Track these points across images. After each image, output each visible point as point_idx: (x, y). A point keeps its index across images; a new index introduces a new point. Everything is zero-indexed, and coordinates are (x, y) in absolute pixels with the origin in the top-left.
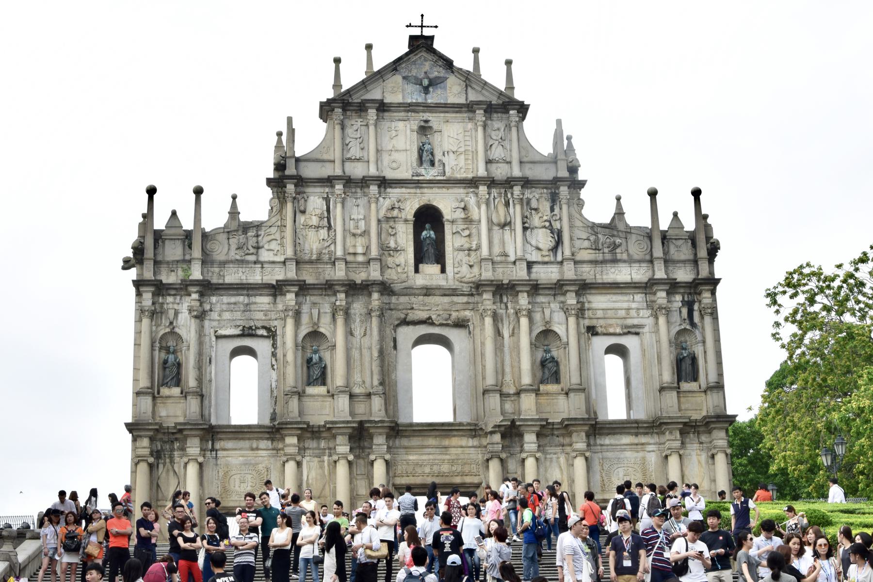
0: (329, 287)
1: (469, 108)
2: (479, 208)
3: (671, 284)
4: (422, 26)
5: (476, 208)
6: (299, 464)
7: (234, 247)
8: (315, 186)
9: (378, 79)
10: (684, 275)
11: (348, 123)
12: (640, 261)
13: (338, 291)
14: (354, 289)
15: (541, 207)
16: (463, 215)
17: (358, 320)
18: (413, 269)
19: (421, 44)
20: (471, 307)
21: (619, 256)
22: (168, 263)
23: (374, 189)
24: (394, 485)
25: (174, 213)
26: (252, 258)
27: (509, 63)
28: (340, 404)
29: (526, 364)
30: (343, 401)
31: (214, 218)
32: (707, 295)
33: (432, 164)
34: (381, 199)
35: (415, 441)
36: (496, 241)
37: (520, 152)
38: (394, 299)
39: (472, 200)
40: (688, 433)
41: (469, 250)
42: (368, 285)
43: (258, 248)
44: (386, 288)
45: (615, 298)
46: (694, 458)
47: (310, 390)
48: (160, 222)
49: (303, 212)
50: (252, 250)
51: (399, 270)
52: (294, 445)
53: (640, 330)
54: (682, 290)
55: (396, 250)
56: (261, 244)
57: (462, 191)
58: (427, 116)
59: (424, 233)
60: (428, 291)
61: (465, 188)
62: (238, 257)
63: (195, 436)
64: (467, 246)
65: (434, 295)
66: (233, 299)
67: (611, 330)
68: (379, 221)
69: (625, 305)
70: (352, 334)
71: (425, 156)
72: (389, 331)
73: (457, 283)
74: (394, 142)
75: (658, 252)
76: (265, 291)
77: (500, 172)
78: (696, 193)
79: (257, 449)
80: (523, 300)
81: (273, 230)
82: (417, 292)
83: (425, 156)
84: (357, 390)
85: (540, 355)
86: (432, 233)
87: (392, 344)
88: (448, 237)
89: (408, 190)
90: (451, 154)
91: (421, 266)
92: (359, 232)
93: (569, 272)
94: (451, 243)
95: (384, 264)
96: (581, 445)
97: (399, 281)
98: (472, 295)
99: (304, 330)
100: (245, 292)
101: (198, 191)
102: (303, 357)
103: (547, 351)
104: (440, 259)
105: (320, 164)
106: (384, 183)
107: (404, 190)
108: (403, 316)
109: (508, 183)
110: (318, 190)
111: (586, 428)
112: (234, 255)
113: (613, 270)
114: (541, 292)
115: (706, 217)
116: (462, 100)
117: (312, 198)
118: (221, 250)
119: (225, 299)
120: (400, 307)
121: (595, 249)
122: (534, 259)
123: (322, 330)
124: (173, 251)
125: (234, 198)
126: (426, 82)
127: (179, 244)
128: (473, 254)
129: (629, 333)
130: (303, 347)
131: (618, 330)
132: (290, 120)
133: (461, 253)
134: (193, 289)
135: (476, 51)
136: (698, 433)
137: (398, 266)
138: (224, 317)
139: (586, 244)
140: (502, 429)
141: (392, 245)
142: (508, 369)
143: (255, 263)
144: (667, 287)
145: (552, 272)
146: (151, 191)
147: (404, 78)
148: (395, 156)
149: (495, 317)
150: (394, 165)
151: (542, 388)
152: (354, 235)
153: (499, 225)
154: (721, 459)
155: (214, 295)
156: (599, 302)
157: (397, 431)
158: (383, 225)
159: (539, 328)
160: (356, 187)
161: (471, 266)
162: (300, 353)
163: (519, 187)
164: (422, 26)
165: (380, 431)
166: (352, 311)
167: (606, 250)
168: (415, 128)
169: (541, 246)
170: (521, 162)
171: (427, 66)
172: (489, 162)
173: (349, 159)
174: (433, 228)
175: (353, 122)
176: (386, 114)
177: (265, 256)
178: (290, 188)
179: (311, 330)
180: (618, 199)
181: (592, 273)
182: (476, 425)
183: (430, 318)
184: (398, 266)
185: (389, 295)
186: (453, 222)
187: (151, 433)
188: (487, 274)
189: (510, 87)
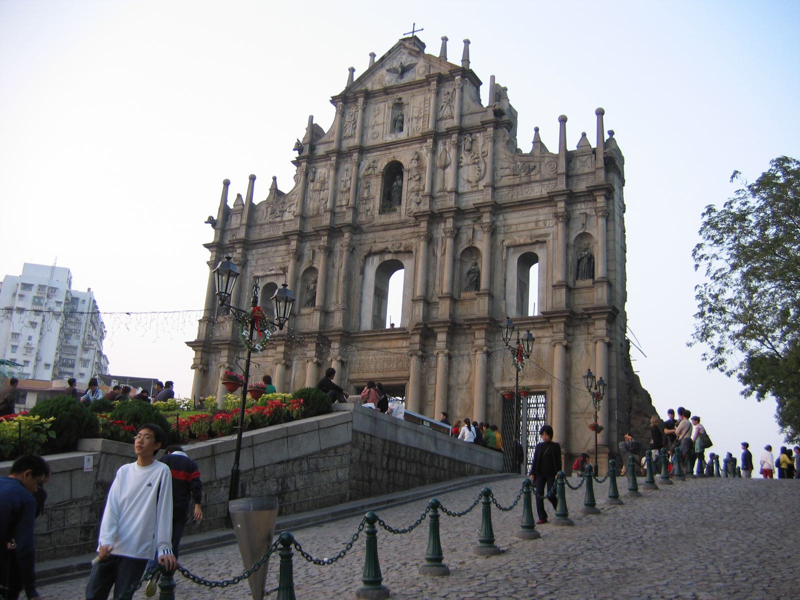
0: (317, 234)
1: (427, 81)
3: (568, 194)
4: (413, 32)
6: (288, 367)
7: (269, 212)
8: (322, 161)
9: (370, 76)
10: (582, 186)
11: (347, 111)
12: (549, 180)
13: (323, 235)
14: (334, 232)
15: (474, 148)
16: (416, 165)
17: (338, 255)
18: (377, 211)
19: (412, 45)
20: (416, 235)
21: (533, 178)
22: (232, 229)
23: (355, 156)
24: (348, 380)
25: (239, 196)
26: (278, 219)
27: (467, 42)
28: (314, 319)
29: (447, 277)
30: (317, 317)
31: (261, 195)
32: (601, 201)
33: (401, 130)
34: (362, 163)
35: (368, 345)
36: (439, 180)
37: (461, 108)
38: (363, 237)
39: (424, 151)
40: (580, 326)
41: (419, 190)
42: (340, 228)
43: (283, 212)
44: (356, 228)
45: (526, 213)
46: (583, 348)
47: (305, 311)
48: (231, 204)
49: (313, 181)
50: (279, 214)
52: (282, 353)
53: (547, 239)
54: (582, 199)
55: (368, 199)
56: (285, 209)
57: (418, 146)
58: (400, 95)
59: (395, 184)
60: (386, 227)
61: (420, 143)
62: (271, 220)
63: (225, 349)
64: (416, 188)
65: (390, 230)
66: (264, 250)
67: (522, 242)
68: (358, 179)
69: (534, 218)
70: (333, 266)
71: (398, 124)
72: (358, 262)
73: (407, 218)
74: (376, 118)
75: (562, 169)
76: (283, 242)
77: (444, 126)
78: (600, 113)
79: (267, 356)
80: (450, 224)
81: (294, 197)
82: (379, 228)
83: (398, 124)
84: (332, 308)
85: (468, 267)
87: (359, 271)
88: (405, 183)
89: (381, 153)
90: (415, 121)
92: (345, 189)
93: (486, 197)
94: (408, 185)
96: (481, 342)
98: (417, 226)
99: (304, 267)
100: (271, 244)
101: (253, 178)
102: (302, 287)
103: (476, 264)
105: (327, 145)
106: (362, 150)
107: (378, 153)
108: (369, 249)
109: (448, 133)
110: (324, 163)
111: (485, 326)
112: (269, 219)
113: (527, 190)
114: (467, 216)
115: (611, 133)
116: (424, 78)
117: (319, 170)
118: (263, 217)
119: (260, 251)
120: (367, 242)
121: (514, 175)
122: (466, 190)
123: (315, 266)
124: (235, 221)
125: (275, 179)
126: (400, 70)
127: (239, 215)
128: (421, 193)
129: (538, 242)
130: (305, 280)
131: (529, 241)
132: (311, 118)
133: (413, 194)
134: (237, 246)
135: (445, 39)
136: (588, 325)
137: (368, 211)
138: (259, 263)
139: (507, 172)
140: (420, 331)
141: (365, 195)
142: (437, 283)
143: (280, 222)
144: (564, 198)
145: (478, 199)
146: (227, 183)
147: (387, 70)
148: (377, 129)
149: (430, 240)
150: (375, 135)
151: (463, 295)
152: (342, 192)
153: (440, 168)
154: (600, 346)
155: (253, 249)
156: (514, 218)
157: (349, 337)
159: (464, 245)
160: (347, 157)
162: (299, 285)
163: (456, 135)
164: (413, 32)
165: (334, 338)
166: (336, 249)
167: (523, 174)
168: (391, 105)
169: (470, 179)
170: (461, 116)
171: (404, 57)
172: (437, 120)
173: (345, 137)
175: (351, 110)
176: (373, 99)
177: (288, 216)
178: (304, 164)
179: (309, 266)
180: (537, 130)
181: (510, 195)
182: (404, 329)
183: (387, 248)
184: (368, 211)
185: (360, 234)
186: (409, 171)
187: (201, 348)
188: (425, 207)
189: (466, 59)
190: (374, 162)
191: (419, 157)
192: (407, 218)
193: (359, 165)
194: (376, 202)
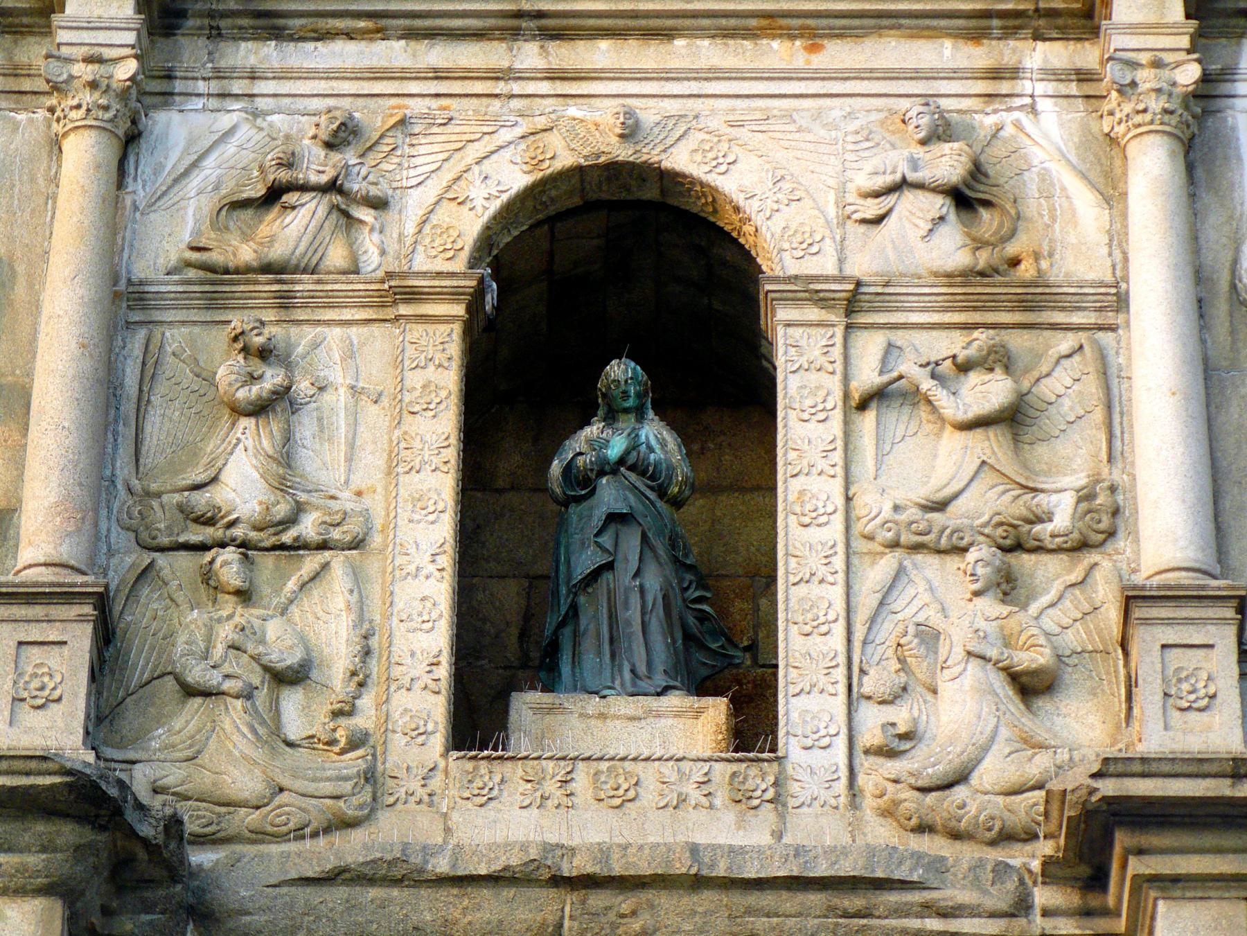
2: (1112, 192)
5: (1086, 206)
16: (950, 248)
39: (1041, 134)
51: (298, 714)
55: (275, 541)
73: (881, 833)
86: (656, 437)
89: (437, 55)
91: (526, 706)
95: (140, 664)
97: (290, 810)
104: (727, 658)
141: (242, 487)
158: (175, 338)
161: (1031, 687)
174: (668, 400)
186: (854, 303)
190: (342, 136)
191: (977, 171)
192: (881, 833)
193: (130, 142)
194: (402, 598)
